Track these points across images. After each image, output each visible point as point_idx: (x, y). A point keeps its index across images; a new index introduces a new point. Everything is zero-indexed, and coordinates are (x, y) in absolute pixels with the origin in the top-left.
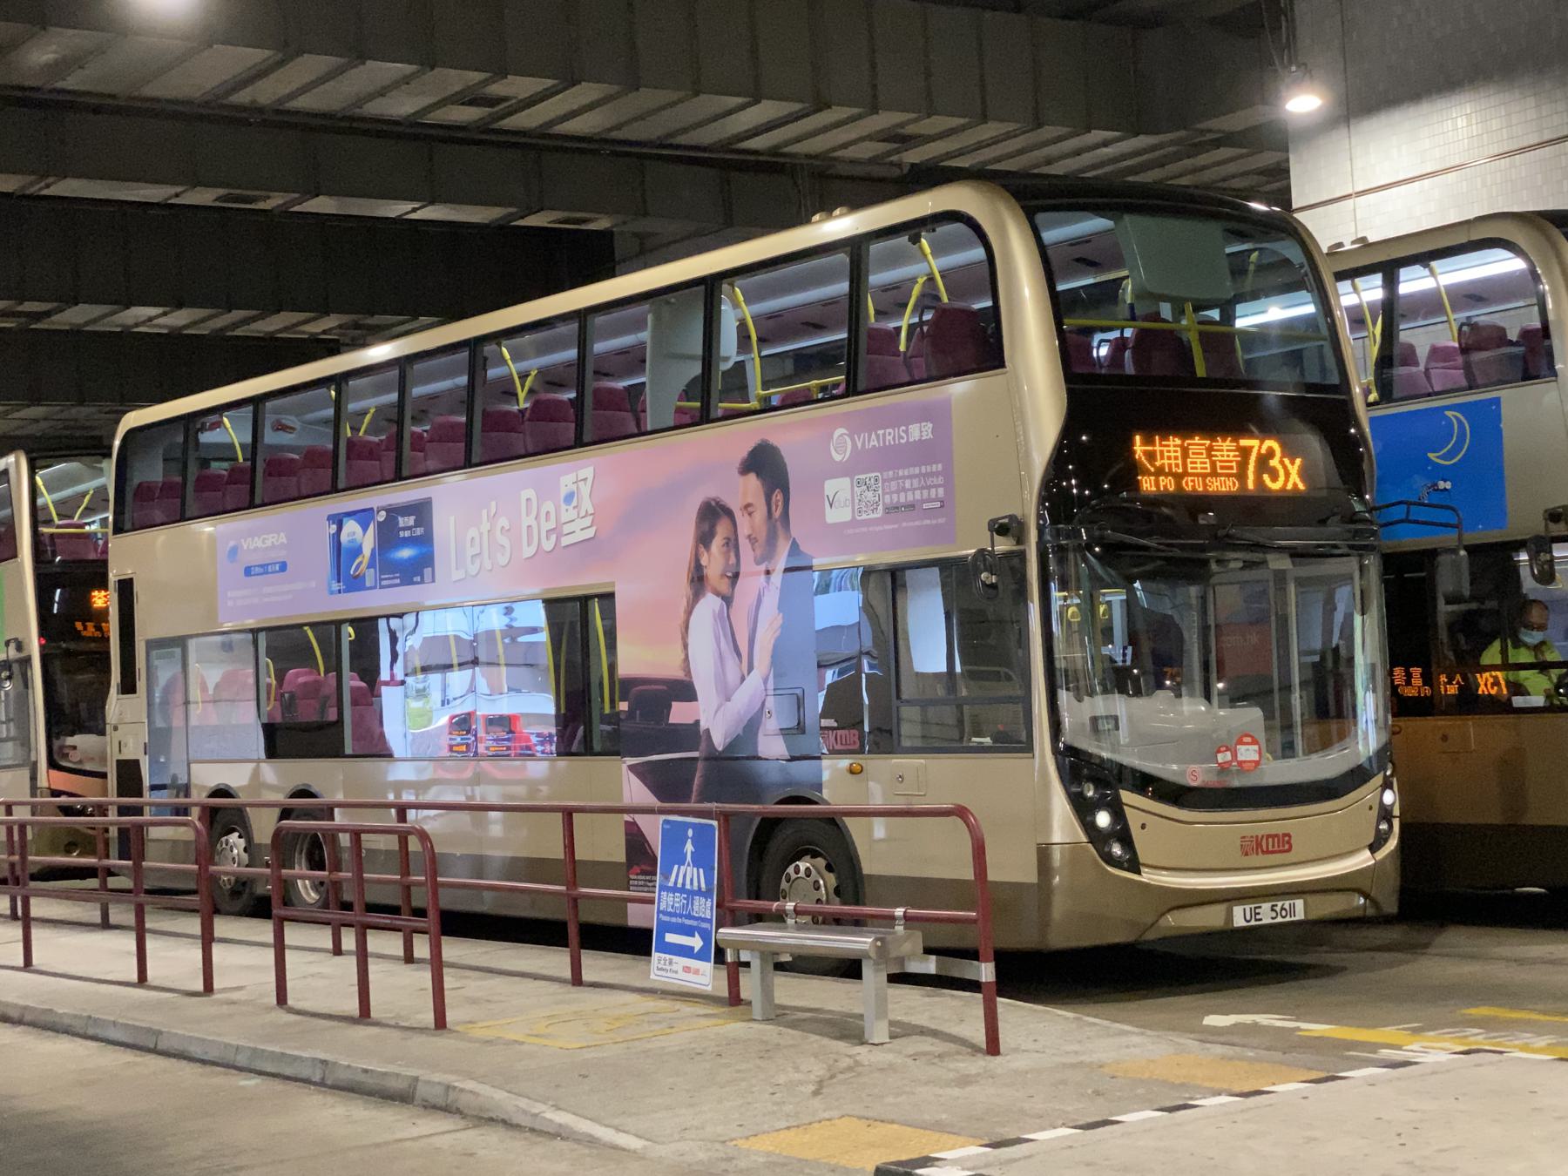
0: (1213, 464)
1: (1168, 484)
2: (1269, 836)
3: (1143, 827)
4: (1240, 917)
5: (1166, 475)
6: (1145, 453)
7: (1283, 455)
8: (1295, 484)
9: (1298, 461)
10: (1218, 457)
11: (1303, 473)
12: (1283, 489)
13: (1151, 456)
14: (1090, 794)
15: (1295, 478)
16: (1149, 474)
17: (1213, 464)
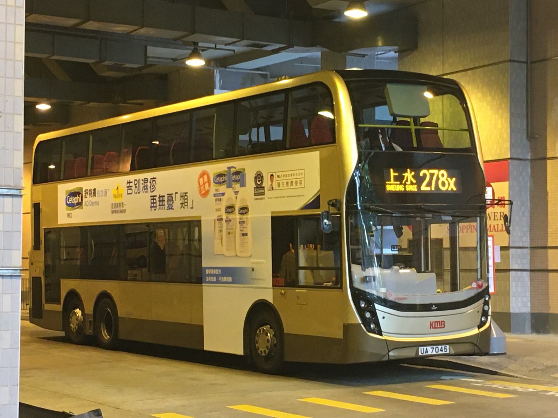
2: (435, 322)
3: (384, 318)
4: (422, 351)
9: (454, 179)
12: (447, 190)
14: (363, 305)
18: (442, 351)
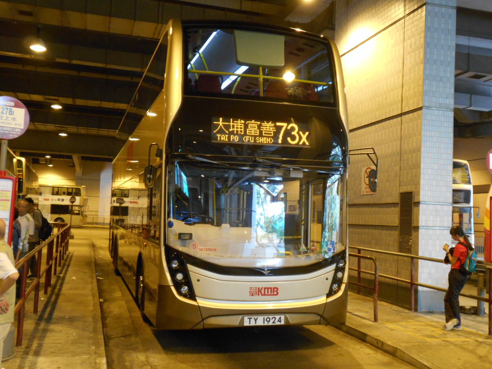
0: (261, 132)
1: (235, 139)
2: (265, 288)
4: (247, 322)
5: (235, 135)
6: (222, 124)
7: (299, 130)
8: (304, 143)
9: (307, 133)
10: (264, 129)
11: (308, 138)
13: (227, 127)
14: (174, 266)
15: (304, 139)
16: (225, 133)
17: (261, 132)
18: (280, 321)
